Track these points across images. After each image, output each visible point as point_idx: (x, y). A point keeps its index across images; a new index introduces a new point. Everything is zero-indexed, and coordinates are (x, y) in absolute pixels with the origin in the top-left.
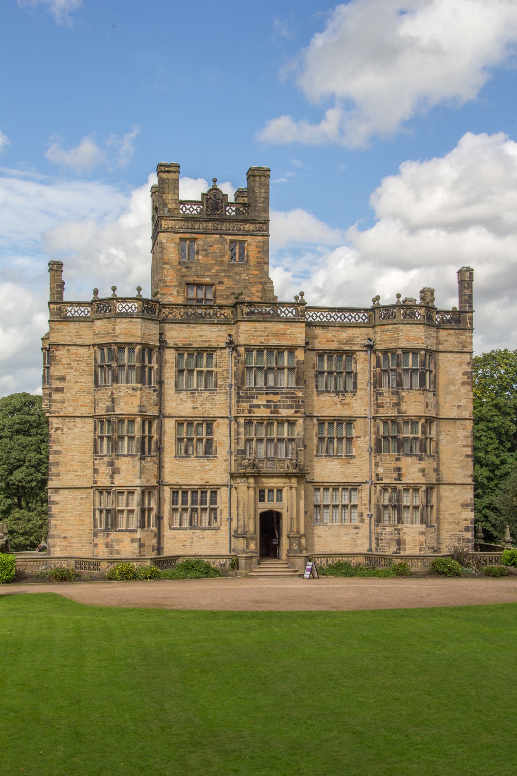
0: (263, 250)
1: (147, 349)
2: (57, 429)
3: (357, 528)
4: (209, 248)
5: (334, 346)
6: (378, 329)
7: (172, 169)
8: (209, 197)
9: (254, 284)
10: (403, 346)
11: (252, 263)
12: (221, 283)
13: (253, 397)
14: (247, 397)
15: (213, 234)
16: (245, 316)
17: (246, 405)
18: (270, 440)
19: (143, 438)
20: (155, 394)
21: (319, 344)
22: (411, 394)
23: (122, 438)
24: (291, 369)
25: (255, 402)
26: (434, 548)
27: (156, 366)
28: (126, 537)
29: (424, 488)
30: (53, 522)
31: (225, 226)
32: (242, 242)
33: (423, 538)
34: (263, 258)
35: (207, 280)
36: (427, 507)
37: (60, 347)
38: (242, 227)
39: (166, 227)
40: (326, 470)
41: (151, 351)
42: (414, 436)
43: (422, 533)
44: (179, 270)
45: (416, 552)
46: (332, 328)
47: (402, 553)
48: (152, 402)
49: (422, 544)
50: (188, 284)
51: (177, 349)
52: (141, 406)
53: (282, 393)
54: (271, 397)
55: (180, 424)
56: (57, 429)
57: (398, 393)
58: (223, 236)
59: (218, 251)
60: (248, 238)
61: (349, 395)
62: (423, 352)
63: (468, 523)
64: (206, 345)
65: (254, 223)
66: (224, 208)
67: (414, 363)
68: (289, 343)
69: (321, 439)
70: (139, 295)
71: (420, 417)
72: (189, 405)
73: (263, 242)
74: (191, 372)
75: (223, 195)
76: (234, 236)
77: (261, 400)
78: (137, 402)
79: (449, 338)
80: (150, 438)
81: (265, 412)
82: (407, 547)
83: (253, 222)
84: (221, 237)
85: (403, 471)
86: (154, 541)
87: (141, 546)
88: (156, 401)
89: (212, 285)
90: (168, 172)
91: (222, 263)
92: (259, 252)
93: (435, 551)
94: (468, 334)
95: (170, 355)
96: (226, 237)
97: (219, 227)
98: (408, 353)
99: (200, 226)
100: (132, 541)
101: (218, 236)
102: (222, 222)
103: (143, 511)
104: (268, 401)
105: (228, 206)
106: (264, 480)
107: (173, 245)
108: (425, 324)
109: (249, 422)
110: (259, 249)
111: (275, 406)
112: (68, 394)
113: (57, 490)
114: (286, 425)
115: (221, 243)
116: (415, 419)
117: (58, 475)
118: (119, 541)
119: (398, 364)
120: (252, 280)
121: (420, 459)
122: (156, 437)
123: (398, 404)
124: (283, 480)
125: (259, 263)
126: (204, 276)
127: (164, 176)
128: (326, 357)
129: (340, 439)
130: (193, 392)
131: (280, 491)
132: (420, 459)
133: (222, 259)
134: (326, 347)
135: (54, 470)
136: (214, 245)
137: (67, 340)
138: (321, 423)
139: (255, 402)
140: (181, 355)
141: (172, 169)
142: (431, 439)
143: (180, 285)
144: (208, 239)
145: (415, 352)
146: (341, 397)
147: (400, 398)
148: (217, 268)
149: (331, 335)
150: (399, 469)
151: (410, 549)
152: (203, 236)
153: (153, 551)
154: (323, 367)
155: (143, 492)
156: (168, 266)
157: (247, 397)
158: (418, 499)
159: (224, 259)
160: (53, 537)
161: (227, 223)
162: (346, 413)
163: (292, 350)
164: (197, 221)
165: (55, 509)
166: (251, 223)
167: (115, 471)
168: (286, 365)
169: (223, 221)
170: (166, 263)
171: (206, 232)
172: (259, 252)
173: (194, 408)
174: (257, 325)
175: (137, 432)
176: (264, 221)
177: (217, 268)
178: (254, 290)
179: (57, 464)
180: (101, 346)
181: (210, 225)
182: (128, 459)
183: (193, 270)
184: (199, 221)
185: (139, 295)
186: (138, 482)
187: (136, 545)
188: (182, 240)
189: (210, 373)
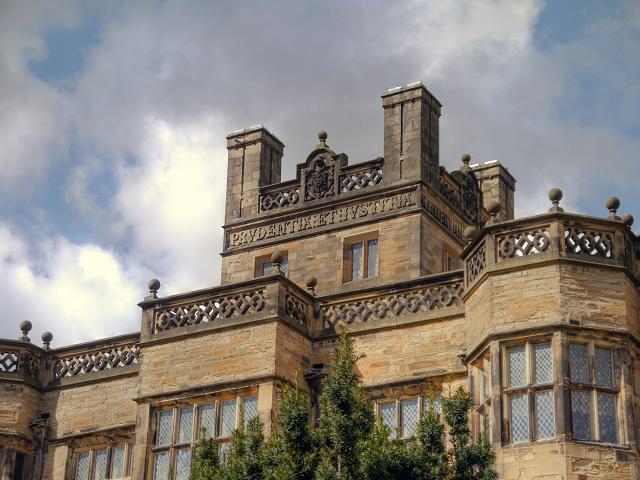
0: (409, 243)
4: (309, 263)
5: (392, 374)
7: (248, 138)
8: (309, 169)
15: (314, 235)
16: (156, 331)
22: (529, 457)
31: (338, 216)
34: (409, 260)
38: (370, 210)
39: (237, 243)
46: (383, 334)
58: (333, 234)
59: (322, 265)
60: (380, 227)
62: (558, 338)
65: (392, 195)
66: (336, 185)
68: (241, 377)
73: (409, 226)
75: (336, 158)
76: (354, 230)
83: (390, 193)
84: (329, 237)
90: (244, 145)
92: (401, 248)
96: (338, 234)
97: (328, 219)
98: (523, 346)
101: (324, 236)
102: (333, 208)
105: (345, 176)
108: (560, 262)
110: (401, 244)
115: (330, 249)
127: (239, 153)
133: (330, 280)
136: (317, 257)
141: (248, 138)
144: (305, 247)
145: (538, 337)
149: (380, 351)
152: (297, 242)
159: (334, 279)
161: (344, 210)
163: (246, 388)
164: (288, 218)
166: (387, 196)
169: (334, 206)
172: (401, 248)
176: (410, 184)
181: (314, 220)
184: (293, 217)
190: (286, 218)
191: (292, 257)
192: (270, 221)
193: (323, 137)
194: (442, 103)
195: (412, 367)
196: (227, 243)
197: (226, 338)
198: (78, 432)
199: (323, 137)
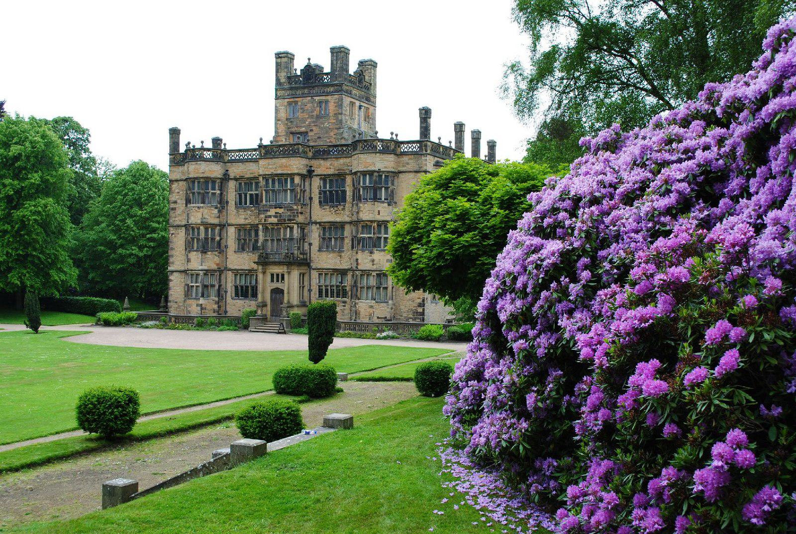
1: (208, 181)
2: (172, 234)
3: (345, 302)
5: (331, 172)
6: (353, 158)
7: (282, 55)
9: (331, 130)
10: (361, 169)
11: (331, 115)
12: (311, 130)
13: (267, 211)
14: (264, 211)
17: (262, 216)
18: (279, 240)
19: (206, 239)
20: (216, 210)
21: (318, 171)
23: (193, 239)
24: (292, 191)
25: (269, 214)
26: (386, 318)
27: (218, 192)
28: (193, 303)
29: (374, 274)
30: (171, 292)
32: (327, 102)
33: (371, 310)
35: (303, 129)
36: (378, 288)
37: (175, 182)
40: (325, 260)
41: (214, 182)
42: (369, 236)
43: (371, 307)
44: (287, 124)
45: (366, 320)
47: (358, 321)
48: (213, 216)
49: (370, 315)
50: (292, 133)
51: (236, 179)
52: (203, 218)
53: (285, 207)
54: (278, 210)
55: (239, 230)
56: (172, 234)
57: (357, 205)
60: (329, 98)
61: (341, 207)
63: (420, 301)
64: (252, 176)
67: (370, 183)
68: (289, 172)
69: (324, 239)
70: (202, 146)
71: (372, 221)
72: (243, 217)
74: (246, 196)
77: (272, 212)
78: (199, 215)
79: (411, 161)
80: (213, 239)
81: (274, 220)
82: (361, 316)
83: (333, 85)
85: (359, 261)
86: (216, 307)
87: (202, 309)
88: (218, 215)
89: (307, 133)
90: (281, 57)
91: (312, 117)
93: (389, 320)
94: (423, 158)
95: (232, 185)
99: (299, 92)
100: (197, 305)
103: (205, 287)
104: (276, 213)
106: (271, 267)
107: (283, 107)
109: (266, 229)
111: (281, 216)
112: (179, 212)
113: (172, 272)
114: (288, 229)
116: (369, 223)
117: (173, 263)
118: (190, 306)
119: (359, 183)
120: (331, 127)
121: (371, 253)
122: (218, 238)
123: (358, 213)
124: (281, 267)
125: (335, 114)
126: (301, 127)
127: (279, 60)
128: (328, 181)
129: (336, 239)
130: (245, 208)
131: (283, 276)
132: (371, 253)
134: (325, 173)
135: (171, 260)
137: (178, 177)
138: (324, 229)
139: (269, 214)
140: (240, 184)
141: (282, 55)
142: (386, 239)
143: (286, 135)
145: (371, 173)
146: (336, 209)
147: (359, 208)
148: (309, 120)
150: (357, 259)
151: (363, 318)
153: (214, 312)
154: (325, 187)
155: (205, 274)
156: (280, 122)
157: (264, 211)
158: (372, 281)
160: (170, 301)
162: (338, 220)
163: (292, 176)
165: (171, 284)
167: (189, 260)
168: (289, 187)
170: (279, 120)
171: (303, 96)
173: (246, 219)
174: (270, 161)
175: (202, 236)
177: (309, 120)
178: (332, 134)
179: (172, 256)
180: (186, 180)
181: (306, 91)
182: (195, 253)
183: (295, 123)
185: (202, 146)
186: (200, 268)
187: (199, 308)
188: (290, 104)
189: (257, 195)
190: (297, 89)
191: (299, 104)
192: (291, 89)
193: (309, 59)
194: (349, 48)
195: (338, 170)
196: (276, 95)
197: (284, 161)
198: (238, 177)
199: (309, 59)
